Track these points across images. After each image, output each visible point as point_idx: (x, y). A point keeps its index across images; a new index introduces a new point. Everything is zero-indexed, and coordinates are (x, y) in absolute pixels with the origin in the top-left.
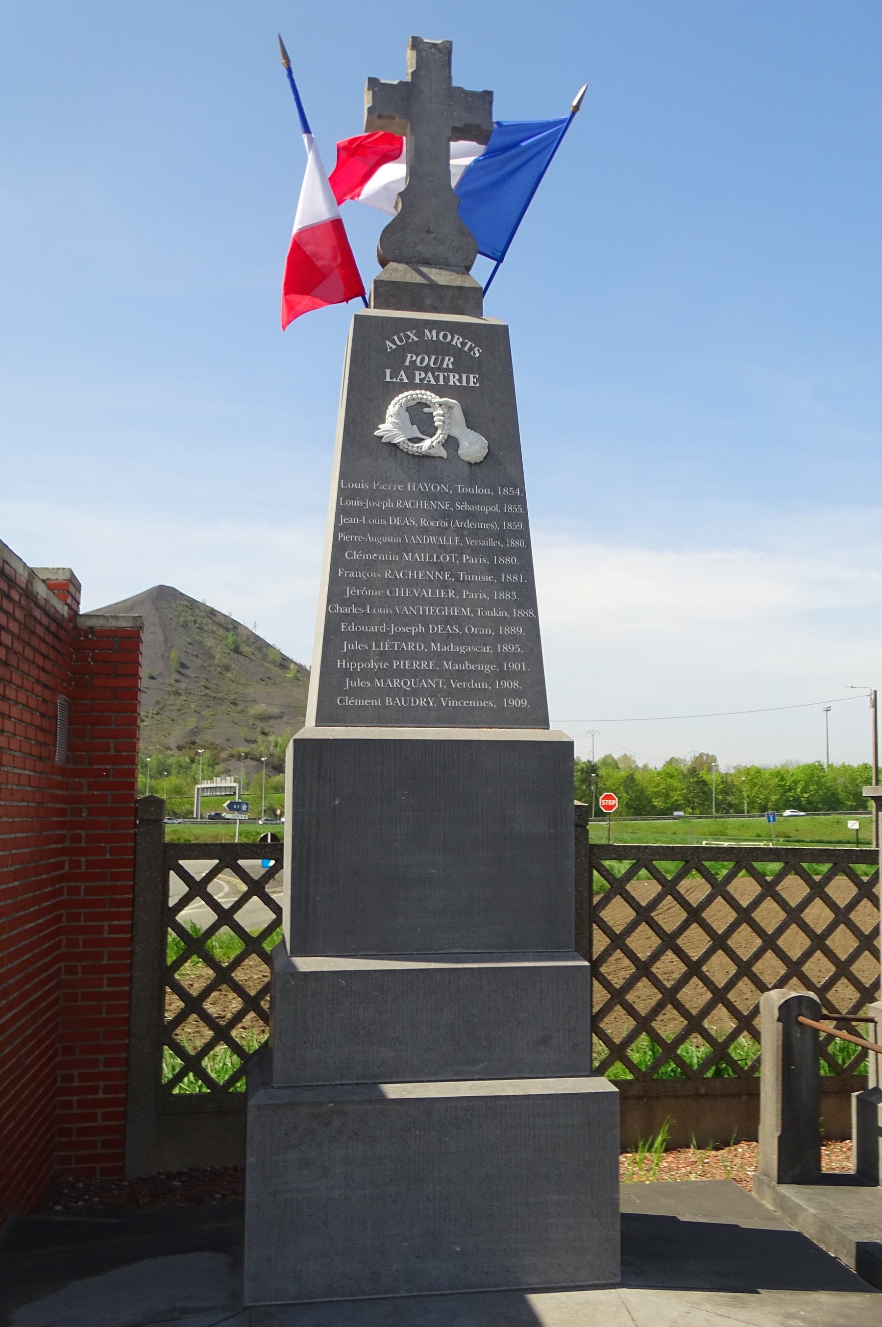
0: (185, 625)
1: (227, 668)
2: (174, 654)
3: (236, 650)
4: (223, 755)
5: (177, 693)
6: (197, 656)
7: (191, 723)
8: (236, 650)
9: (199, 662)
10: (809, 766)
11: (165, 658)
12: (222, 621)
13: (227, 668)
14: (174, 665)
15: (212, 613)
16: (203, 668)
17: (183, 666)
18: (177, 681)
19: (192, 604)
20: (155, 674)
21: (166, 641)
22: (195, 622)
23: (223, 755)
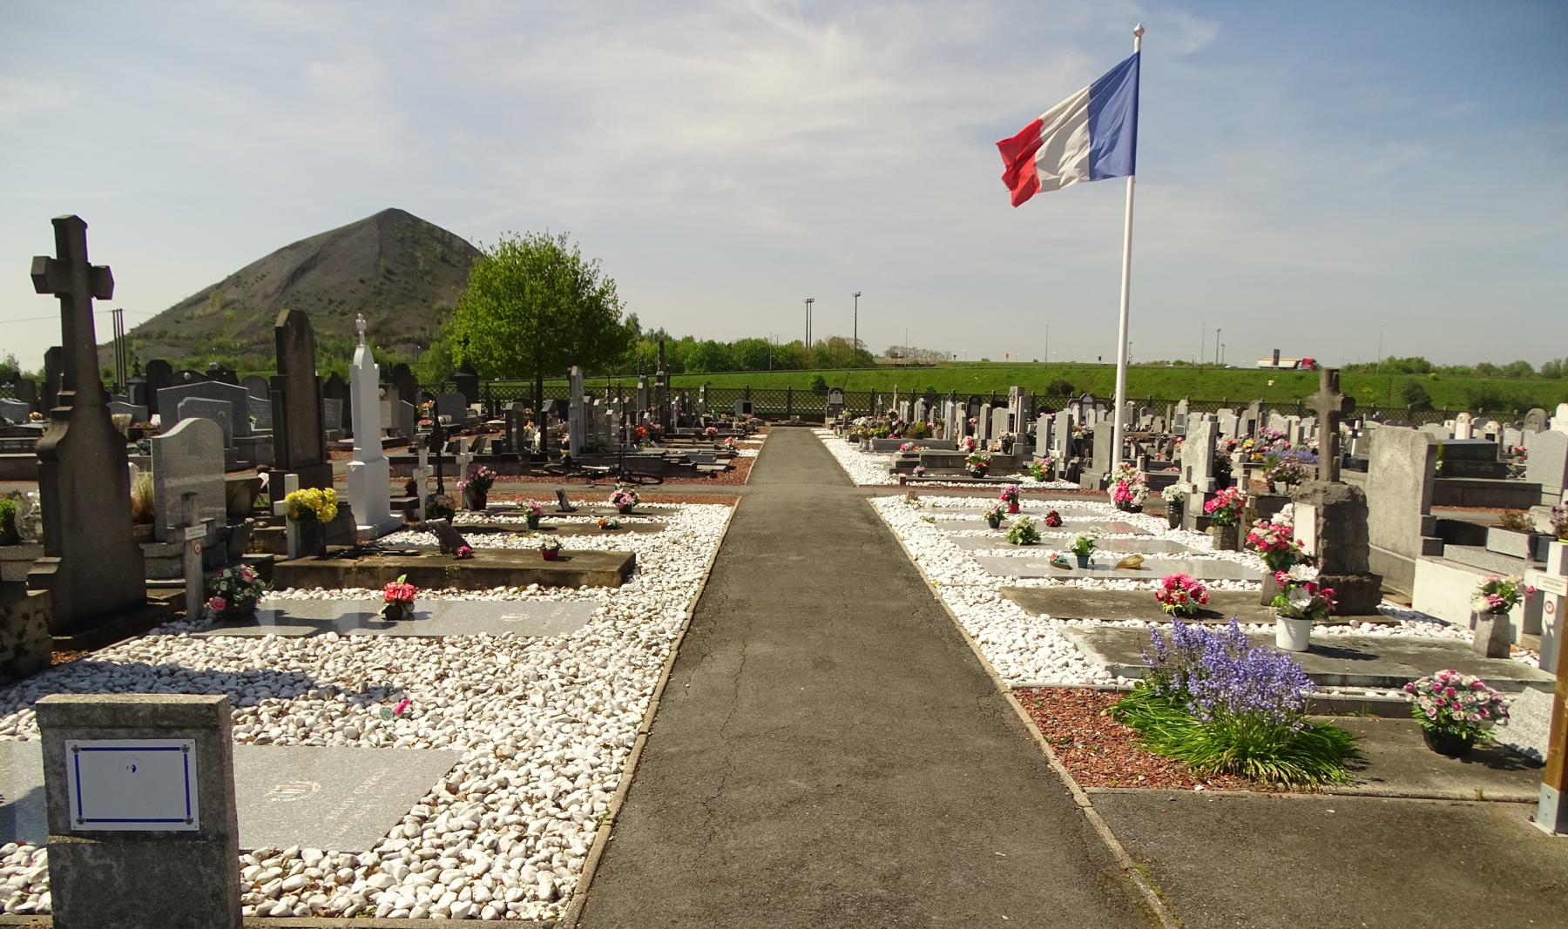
0: (401, 240)
1: (427, 273)
2: (383, 262)
3: (444, 259)
4: (393, 339)
5: (380, 294)
7: (384, 315)
8: (444, 259)
9: (403, 269)
11: (376, 265)
12: (438, 235)
13: (427, 273)
14: (382, 270)
15: (432, 229)
16: (406, 273)
17: (389, 272)
19: (416, 221)
23: (393, 339)
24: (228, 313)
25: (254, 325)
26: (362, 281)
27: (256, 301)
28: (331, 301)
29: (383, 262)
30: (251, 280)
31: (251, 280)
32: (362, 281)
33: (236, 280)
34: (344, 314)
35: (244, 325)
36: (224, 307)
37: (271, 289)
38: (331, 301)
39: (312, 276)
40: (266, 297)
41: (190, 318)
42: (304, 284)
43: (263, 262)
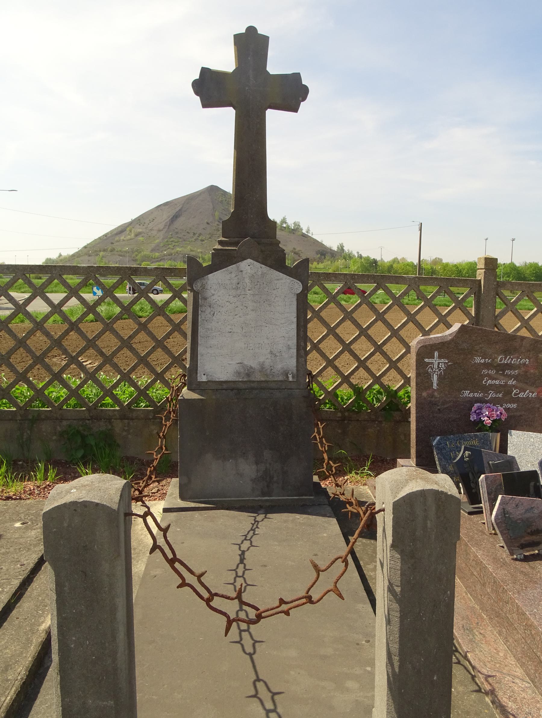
2: (217, 214)
6: (226, 215)
10: (470, 263)
11: (213, 215)
14: (217, 218)
18: (218, 225)
20: (209, 222)
21: (214, 208)
22: (226, 200)
24: (141, 238)
25: (158, 245)
26: (208, 223)
27: (154, 233)
28: (194, 234)
29: (217, 214)
30: (147, 221)
31: (147, 221)
32: (208, 223)
33: (139, 221)
34: (202, 241)
35: (153, 245)
36: (137, 235)
37: (161, 226)
38: (194, 234)
39: (181, 219)
40: (159, 231)
41: (117, 241)
42: (179, 223)
43: (151, 212)
